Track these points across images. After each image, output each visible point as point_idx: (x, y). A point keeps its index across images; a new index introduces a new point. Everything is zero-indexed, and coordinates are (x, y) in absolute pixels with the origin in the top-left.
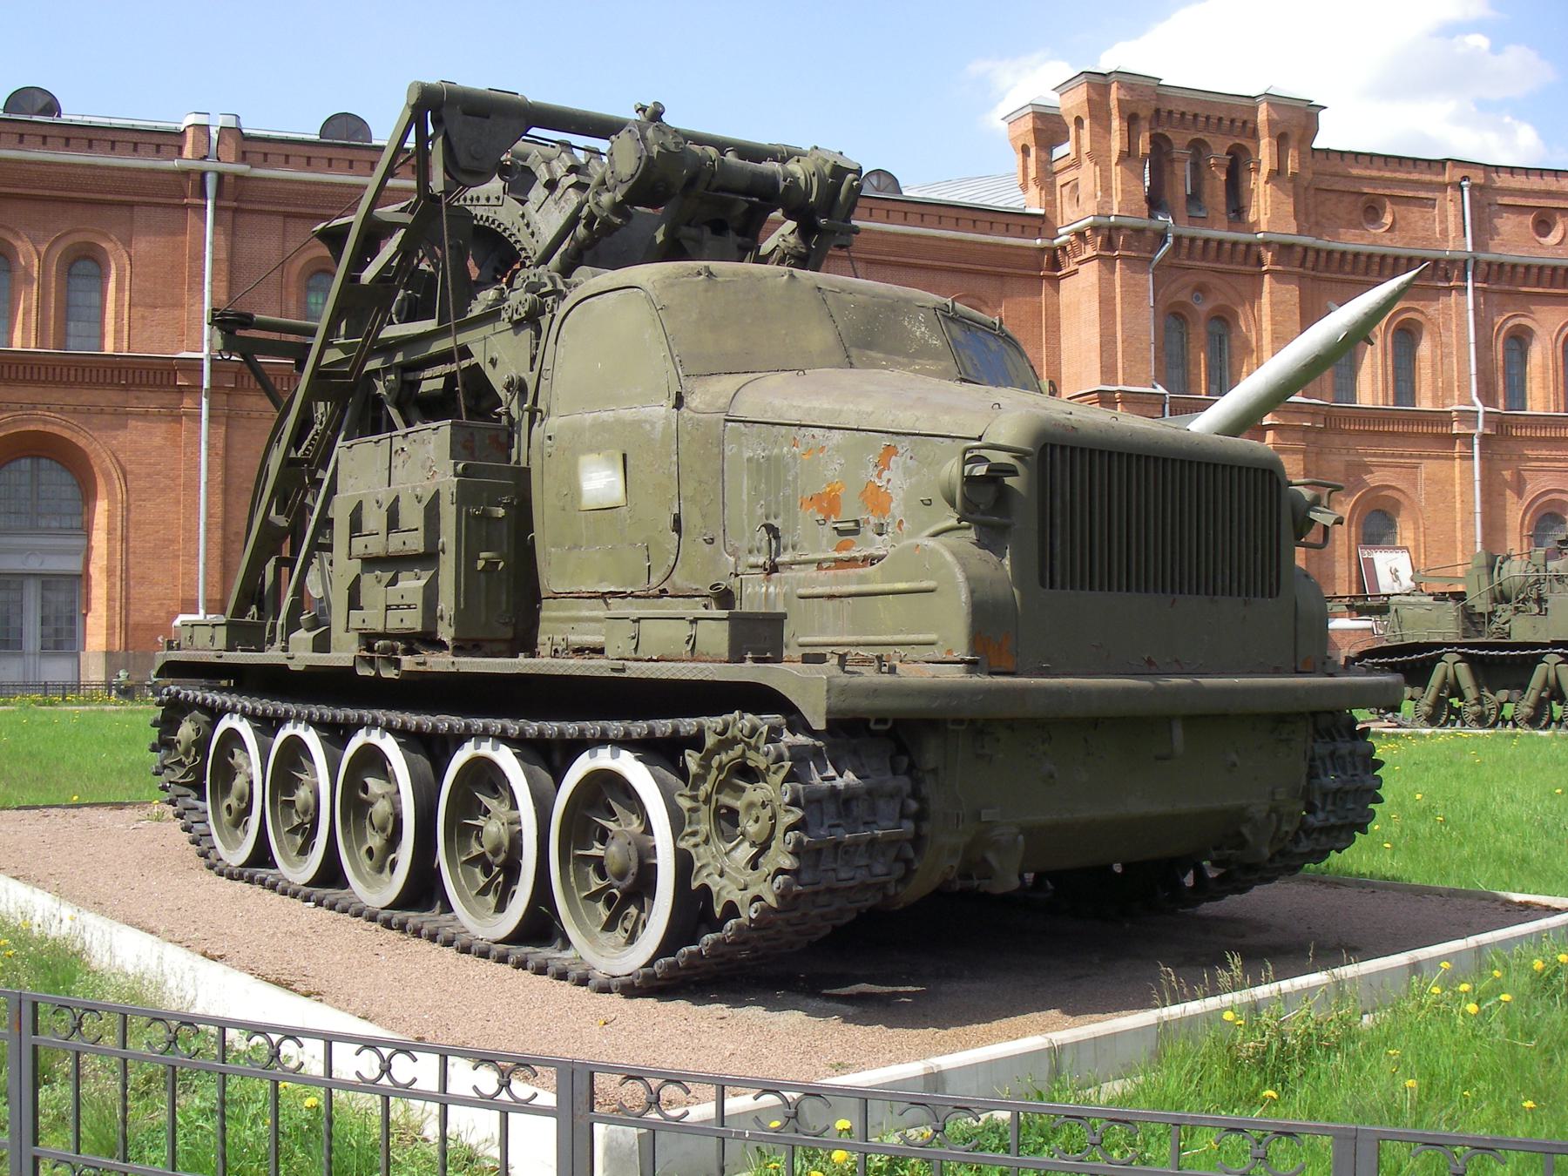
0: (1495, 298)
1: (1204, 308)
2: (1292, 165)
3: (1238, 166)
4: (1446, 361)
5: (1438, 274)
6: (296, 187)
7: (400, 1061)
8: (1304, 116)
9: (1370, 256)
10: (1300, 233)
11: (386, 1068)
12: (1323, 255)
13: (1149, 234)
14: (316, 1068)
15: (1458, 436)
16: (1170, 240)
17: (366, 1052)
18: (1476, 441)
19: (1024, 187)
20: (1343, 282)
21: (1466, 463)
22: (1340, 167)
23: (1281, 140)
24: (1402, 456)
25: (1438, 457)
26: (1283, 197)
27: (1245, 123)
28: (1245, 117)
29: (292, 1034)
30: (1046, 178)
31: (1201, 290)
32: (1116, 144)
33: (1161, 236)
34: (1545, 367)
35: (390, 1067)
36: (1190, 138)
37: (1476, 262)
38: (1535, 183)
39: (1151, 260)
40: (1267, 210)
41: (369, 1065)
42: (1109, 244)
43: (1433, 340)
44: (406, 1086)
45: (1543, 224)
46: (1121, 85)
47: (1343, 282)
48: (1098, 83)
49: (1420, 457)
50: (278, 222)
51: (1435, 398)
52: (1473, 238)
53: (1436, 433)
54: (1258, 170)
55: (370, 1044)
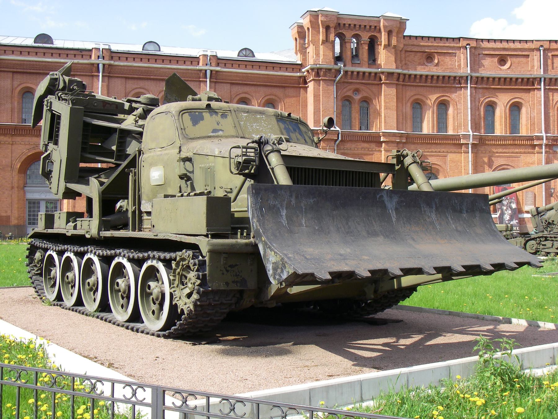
0: (481, 91)
1: (357, 97)
2: (394, 42)
3: (373, 44)
4: (459, 115)
5: (453, 82)
6: (17, 62)
7: (139, 391)
8: (401, 23)
9: (427, 76)
10: (397, 68)
11: (134, 394)
12: (407, 76)
13: (333, 71)
14: (108, 393)
15: (463, 144)
16: (342, 73)
17: (128, 387)
18: (470, 146)
19: (296, 53)
20: (416, 86)
21: (466, 155)
22: (415, 42)
23: (390, 33)
24: (440, 152)
25: (455, 152)
26: (390, 54)
27: (375, 27)
28: (375, 25)
29: (100, 380)
30: (302, 50)
31: (357, 91)
32: (321, 37)
33: (339, 71)
34: (501, 117)
35: (136, 393)
36: (353, 33)
37: (471, 77)
38: (499, 45)
39: (334, 81)
40: (385, 60)
41: (128, 392)
42: (318, 75)
43: (454, 107)
44: (141, 401)
45: (502, 60)
46: (322, 15)
47: (416, 86)
48: (314, 15)
49: (447, 152)
50: (10, 75)
51: (454, 129)
52: (471, 67)
53: (455, 143)
54: (381, 45)
55: (128, 384)
